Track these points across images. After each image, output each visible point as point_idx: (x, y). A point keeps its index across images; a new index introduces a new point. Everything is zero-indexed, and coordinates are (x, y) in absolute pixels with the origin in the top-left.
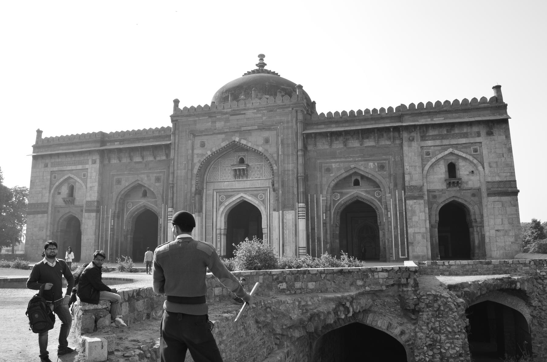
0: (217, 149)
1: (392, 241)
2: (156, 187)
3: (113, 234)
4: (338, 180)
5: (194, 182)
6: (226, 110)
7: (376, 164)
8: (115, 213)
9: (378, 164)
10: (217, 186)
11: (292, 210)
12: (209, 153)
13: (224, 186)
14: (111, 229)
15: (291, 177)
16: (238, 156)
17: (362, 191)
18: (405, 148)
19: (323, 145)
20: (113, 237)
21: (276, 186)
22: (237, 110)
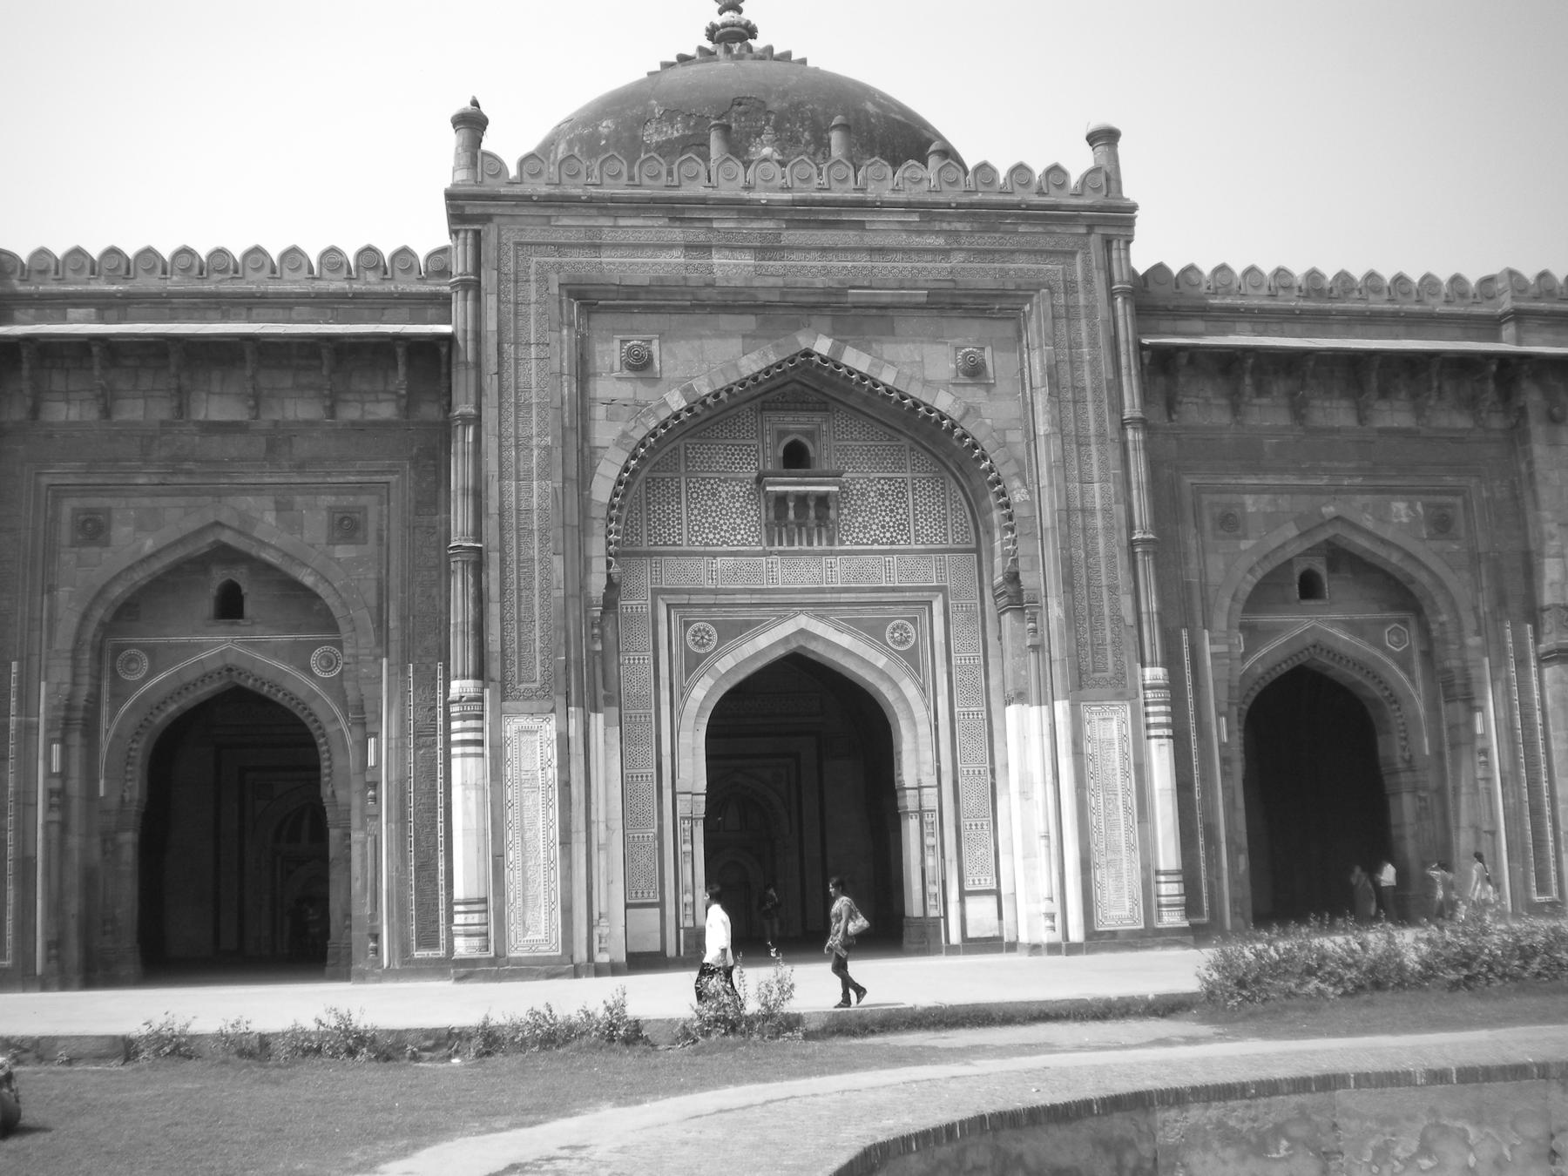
0: (721, 383)
1: (1494, 833)
2: (338, 570)
3: (64, 826)
4: (1268, 567)
5: (597, 547)
6: (762, 196)
7: (1419, 507)
8: (69, 707)
9: (1425, 506)
10: (675, 573)
11: (1120, 696)
12: (677, 402)
13: (716, 573)
14: (51, 793)
15: (1101, 541)
16: (800, 427)
17: (1334, 623)
18: (1539, 450)
19: (1204, 410)
20: (62, 843)
21: (1026, 580)
22: (824, 203)
